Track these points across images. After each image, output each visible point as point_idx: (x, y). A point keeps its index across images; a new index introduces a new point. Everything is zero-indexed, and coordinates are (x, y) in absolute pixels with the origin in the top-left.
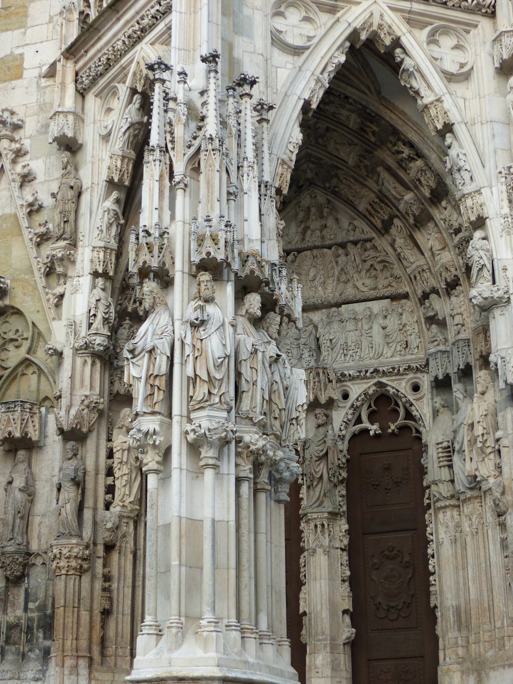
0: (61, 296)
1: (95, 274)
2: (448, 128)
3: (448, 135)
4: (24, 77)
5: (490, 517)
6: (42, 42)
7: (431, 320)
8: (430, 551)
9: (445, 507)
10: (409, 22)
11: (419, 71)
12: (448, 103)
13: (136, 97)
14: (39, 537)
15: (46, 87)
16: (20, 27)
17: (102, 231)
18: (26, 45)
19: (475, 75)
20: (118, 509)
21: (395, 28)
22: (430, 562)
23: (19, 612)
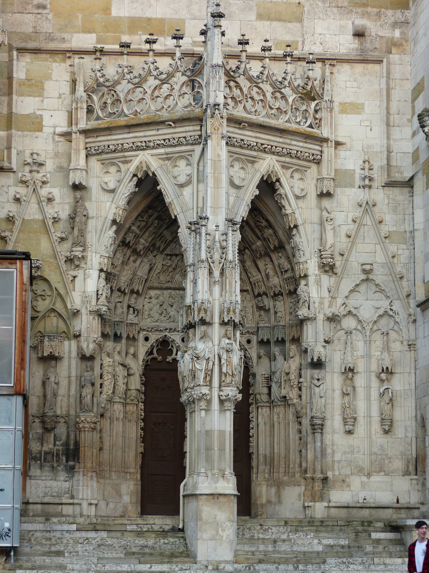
0: (75, 277)
1: (101, 270)
2: (296, 226)
3: (295, 229)
4: (43, 131)
5: (291, 417)
6: (54, 110)
7: (260, 308)
8: (251, 426)
9: (264, 406)
10: (283, 167)
11: (286, 195)
12: (297, 215)
13: (135, 178)
14: (61, 407)
15: (59, 142)
16: (39, 96)
17: (107, 247)
18: (44, 109)
19: (308, 196)
20: (105, 396)
21: (278, 173)
22: (251, 431)
23: (51, 446)
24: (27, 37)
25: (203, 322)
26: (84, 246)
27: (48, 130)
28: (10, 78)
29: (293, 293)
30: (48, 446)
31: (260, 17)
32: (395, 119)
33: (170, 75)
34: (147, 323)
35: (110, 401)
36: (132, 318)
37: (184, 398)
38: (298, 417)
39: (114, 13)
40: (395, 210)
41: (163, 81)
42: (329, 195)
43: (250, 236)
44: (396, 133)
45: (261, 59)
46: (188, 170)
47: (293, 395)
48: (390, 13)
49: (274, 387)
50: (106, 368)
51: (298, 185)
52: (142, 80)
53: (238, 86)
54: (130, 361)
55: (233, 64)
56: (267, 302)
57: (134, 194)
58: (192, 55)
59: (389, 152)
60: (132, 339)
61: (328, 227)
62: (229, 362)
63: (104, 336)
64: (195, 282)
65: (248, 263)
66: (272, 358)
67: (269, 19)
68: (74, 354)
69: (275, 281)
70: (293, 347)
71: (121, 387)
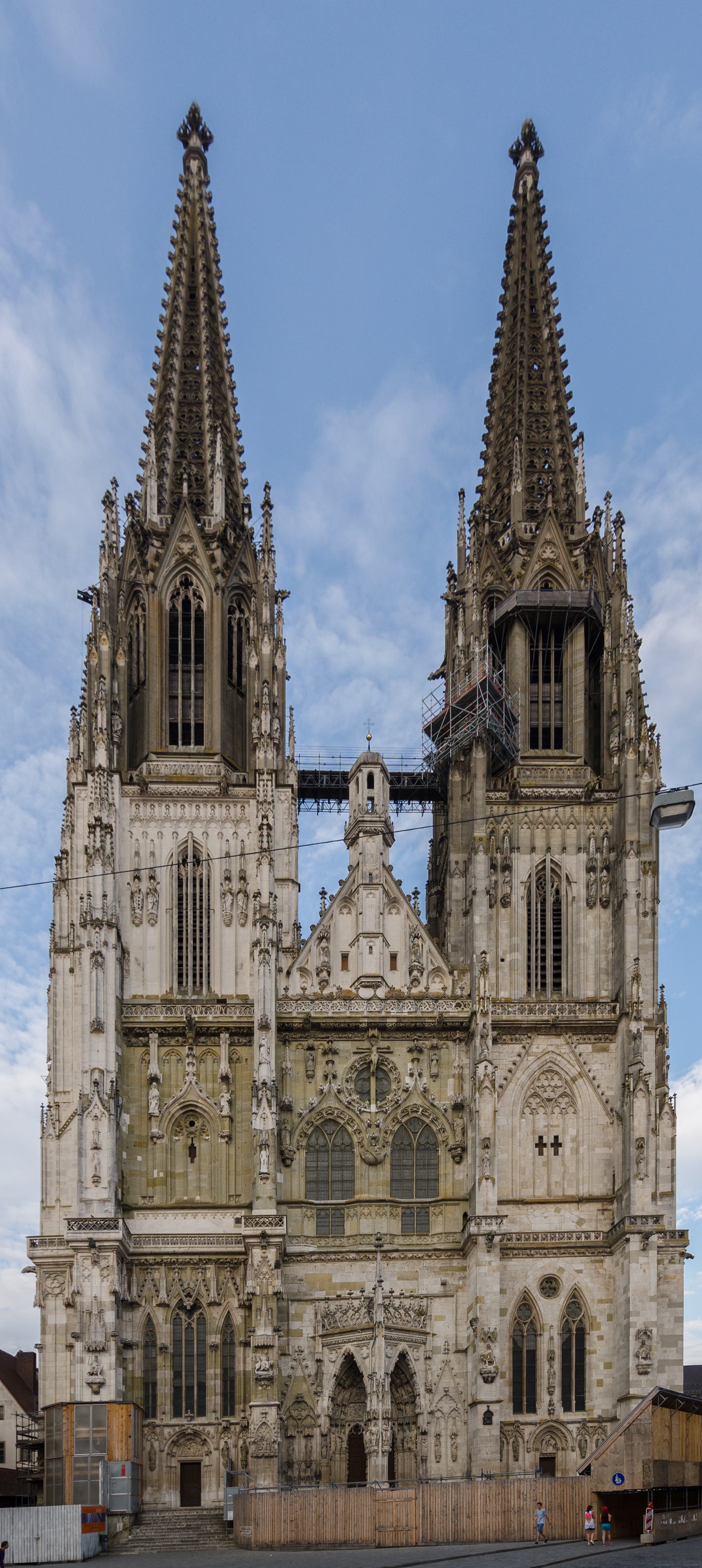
24: (295, 1294)
25: (375, 1418)
26: (322, 1386)
27: (305, 1336)
28: (288, 1313)
29: (413, 1402)
30: (308, 1474)
31: (399, 1279)
32: (459, 1322)
33: (359, 1309)
34: (349, 1418)
35: (334, 1453)
36: (343, 1416)
37: (366, 1451)
38: (416, 1456)
39: (333, 1281)
40: (459, 1363)
41: (356, 1312)
42: (429, 1358)
43: (395, 1378)
44: (460, 1328)
45: (399, 1298)
46: (367, 1351)
47: (413, 1447)
48: (457, 1273)
49: (405, 1444)
50: (333, 1439)
51: (416, 1354)
52: (347, 1311)
53: (389, 1312)
54: (342, 1436)
55: (387, 1302)
56: (402, 1407)
57: (343, 1363)
58: (368, 1298)
59: (457, 1337)
60: (343, 1426)
61: (429, 1372)
62: (386, 1435)
63: (331, 1425)
64: (371, 1401)
65: (394, 1390)
66: (404, 1431)
67: (403, 1279)
68: (318, 1433)
69: (405, 1397)
70: (414, 1426)
71: (339, 1447)
